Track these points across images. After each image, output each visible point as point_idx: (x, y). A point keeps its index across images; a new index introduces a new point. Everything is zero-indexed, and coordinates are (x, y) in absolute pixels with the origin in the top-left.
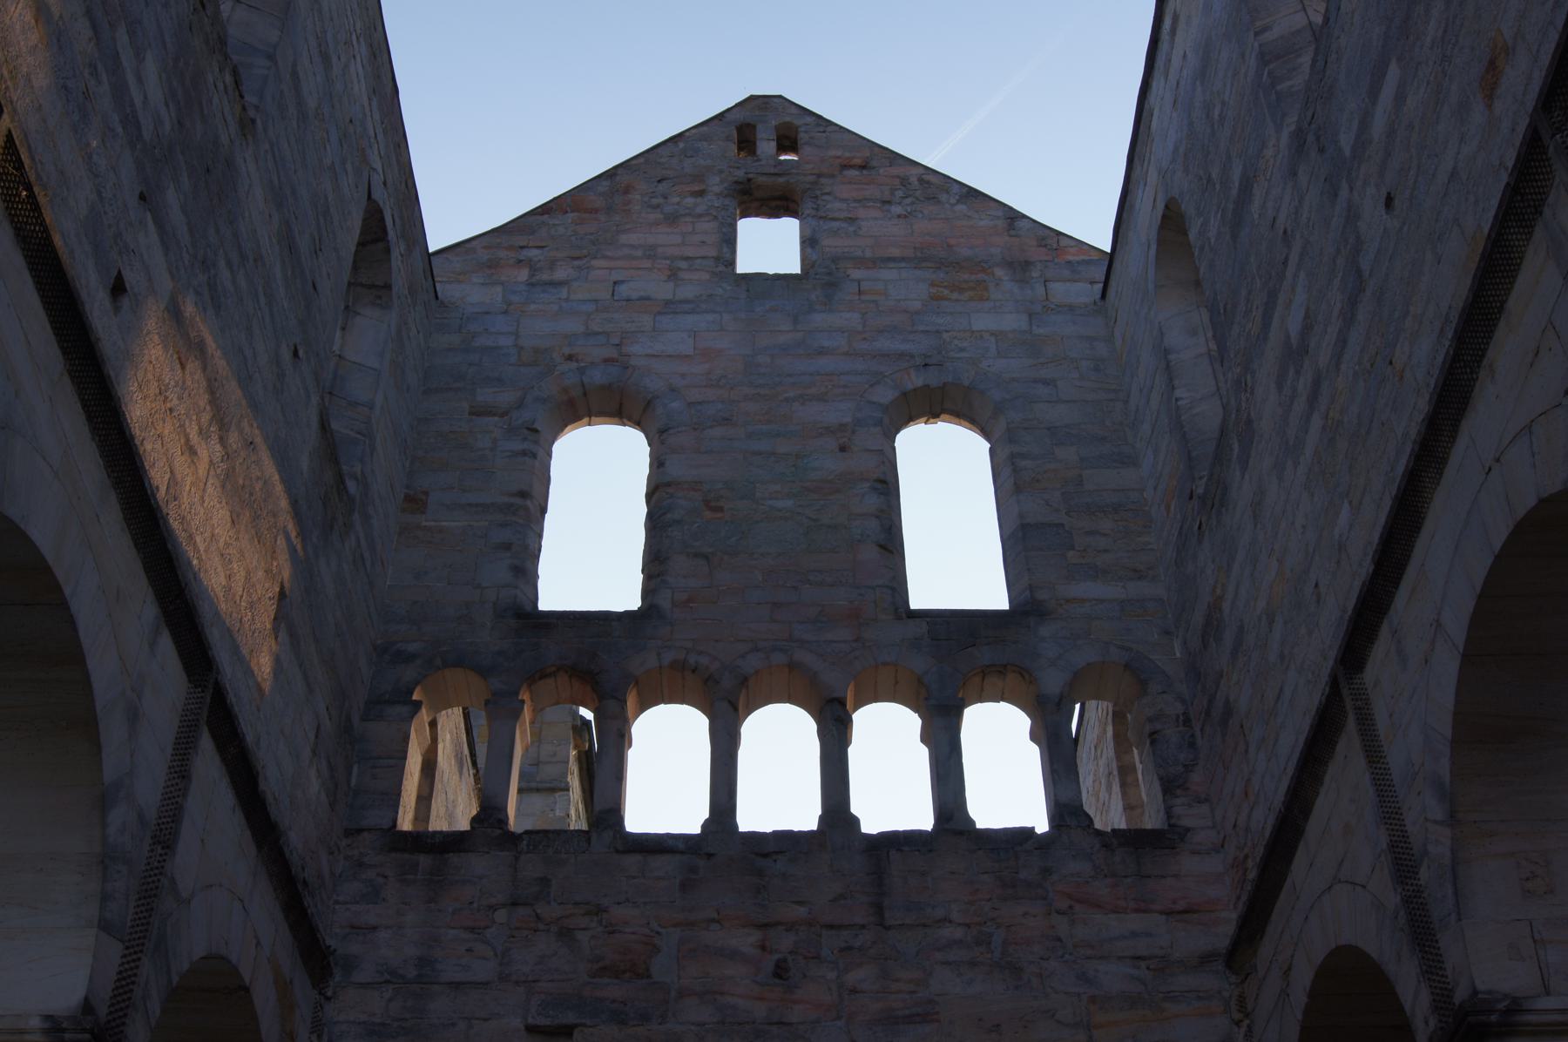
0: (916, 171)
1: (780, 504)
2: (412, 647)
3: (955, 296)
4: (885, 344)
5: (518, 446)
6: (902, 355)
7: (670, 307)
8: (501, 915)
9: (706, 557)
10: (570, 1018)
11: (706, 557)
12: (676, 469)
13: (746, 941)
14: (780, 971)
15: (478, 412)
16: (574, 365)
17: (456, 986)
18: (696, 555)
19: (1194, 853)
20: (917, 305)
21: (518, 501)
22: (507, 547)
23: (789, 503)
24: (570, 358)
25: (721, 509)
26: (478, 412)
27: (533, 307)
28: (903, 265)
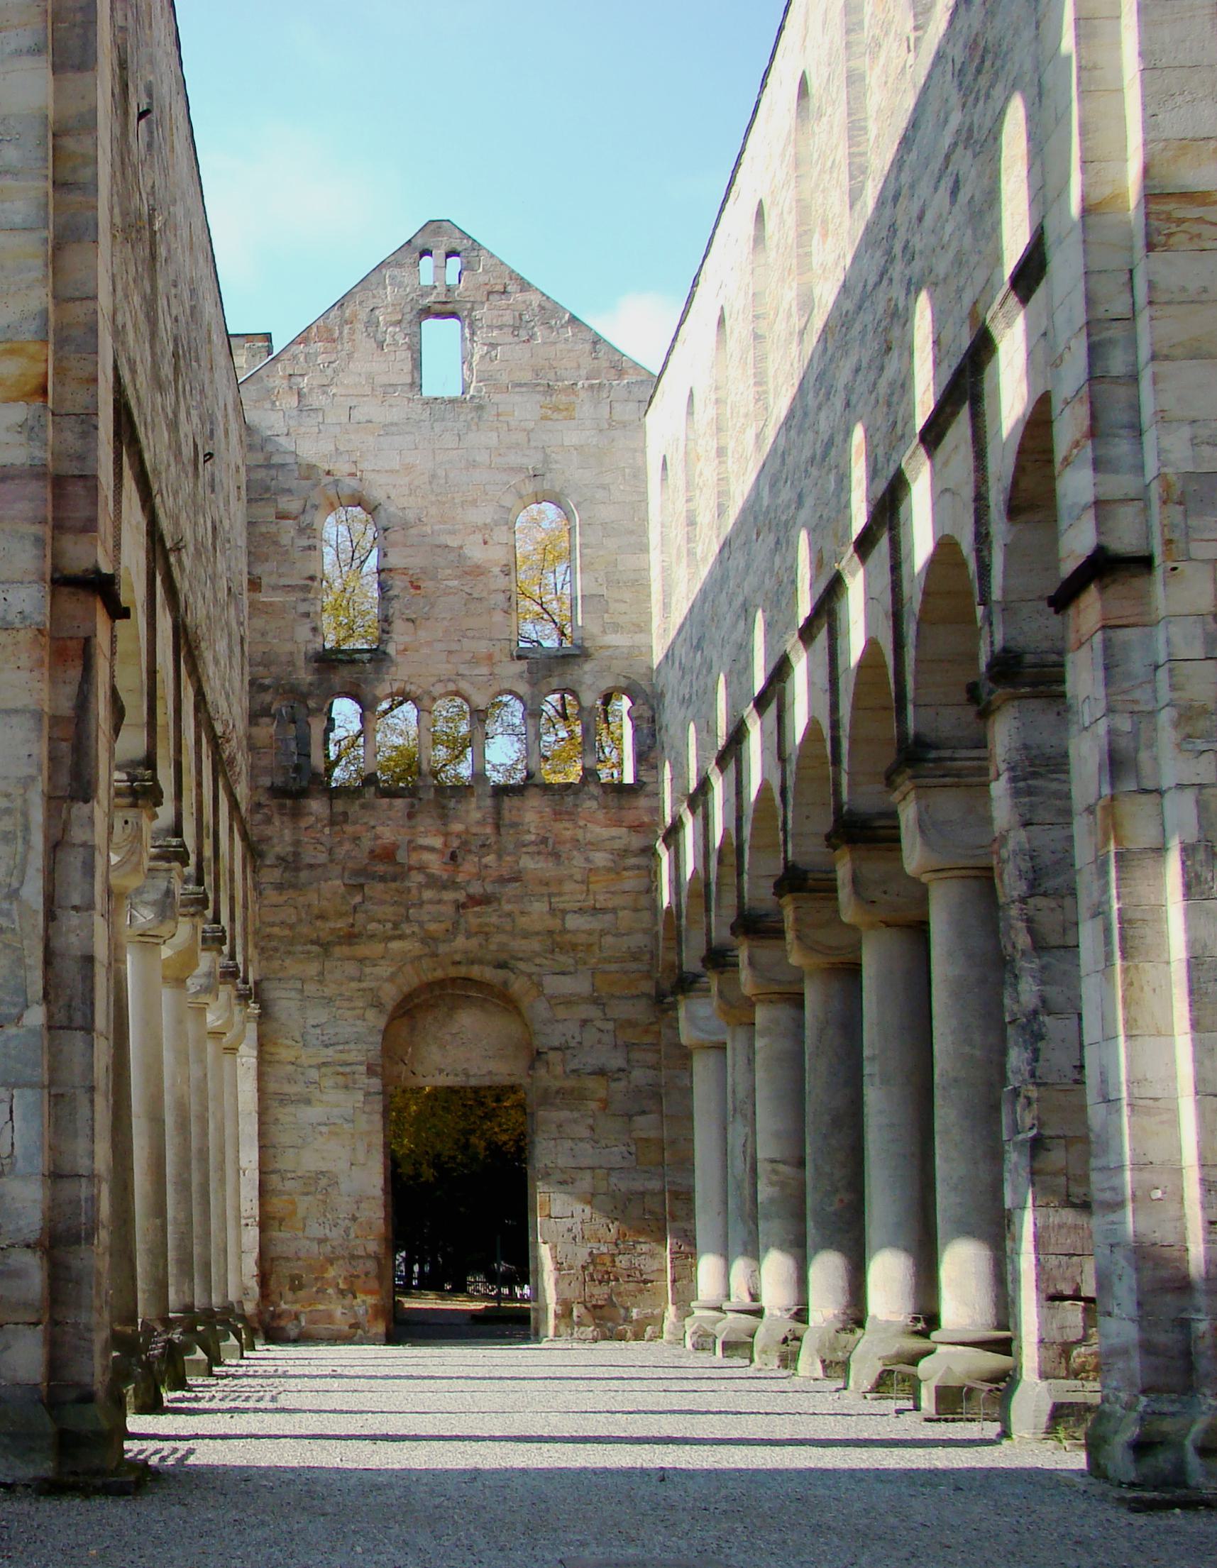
0: (535, 300)
1: (451, 583)
2: (267, 681)
3: (555, 416)
4: (514, 459)
5: (306, 543)
6: (520, 469)
7: (388, 429)
8: (327, 830)
9: (413, 621)
10: (362, 880)
11: (413, 621)
12: (394, 560)
13: (437, 842)
14: (453, 857)
15: (282, 516)
16: (330, 479)
17: (311, 866)
18: (408, 620)
19: (647, 796)
20: (531, 425)
21: (309, 582)
22: (307, 615)
23: (456, 583)
24: (328, 473)
25: (418, 588)
26: (282, 516)
27: (303, 430)
28: (524, 389)
